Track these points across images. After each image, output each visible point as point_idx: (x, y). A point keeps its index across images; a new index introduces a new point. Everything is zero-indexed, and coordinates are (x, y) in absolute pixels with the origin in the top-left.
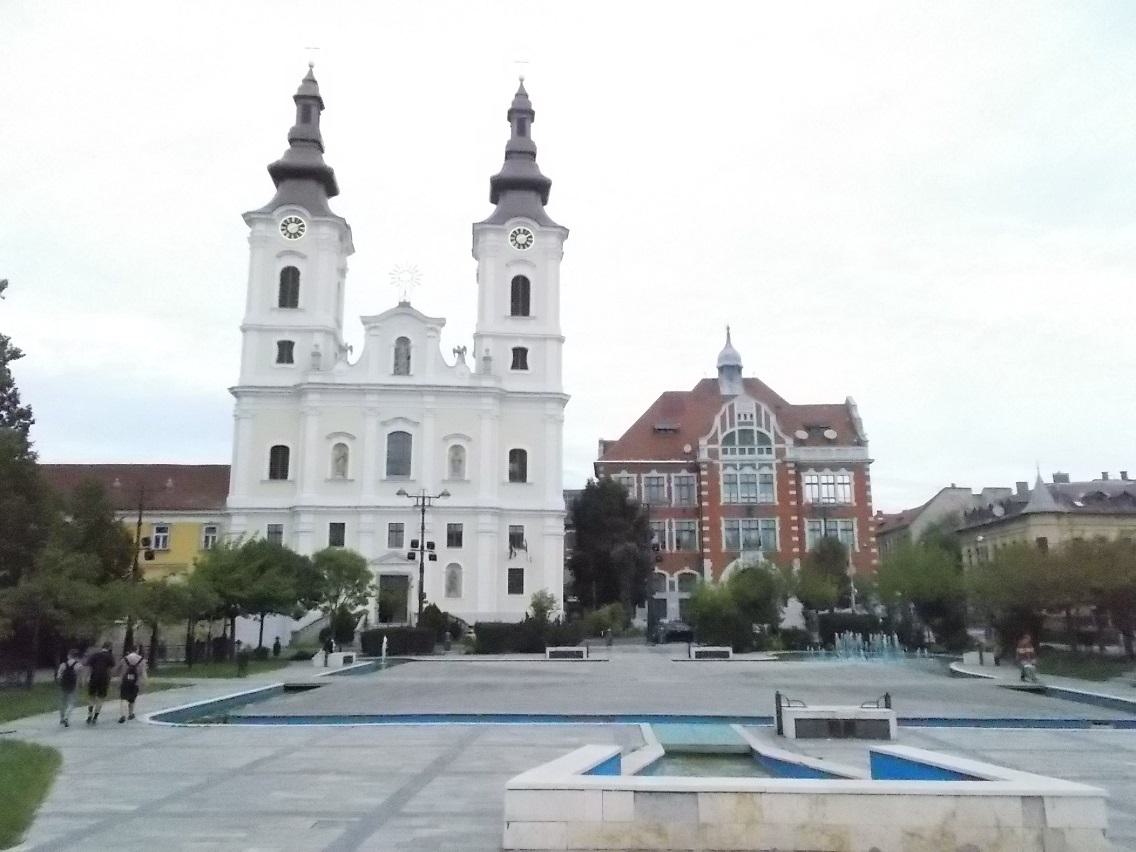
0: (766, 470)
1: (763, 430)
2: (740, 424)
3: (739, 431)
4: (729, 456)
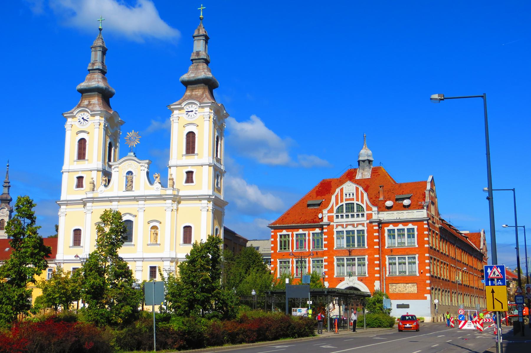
0: (360, 228)
1: (360, 203)
2: (346, 200)
3: (346, 204)
4: (340, 220)
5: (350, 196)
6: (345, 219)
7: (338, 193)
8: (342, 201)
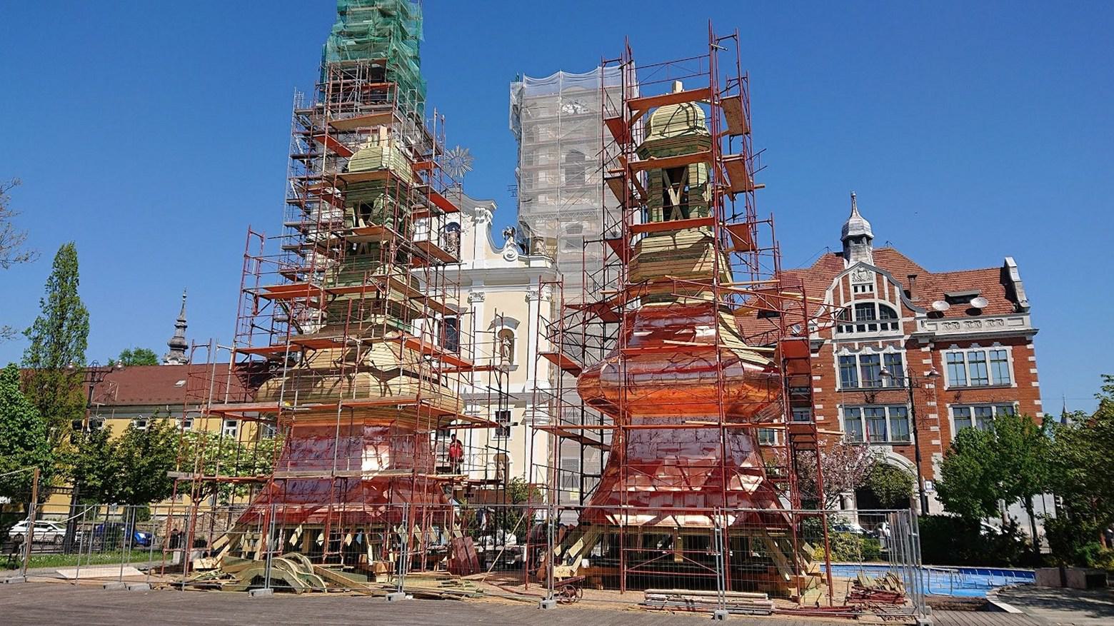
1: (887, 303)
2: (857, 297)
4: (845, 335)
5: (864, 290)
6: (856, 334)
7: (838, 286)
8: (847, 299)
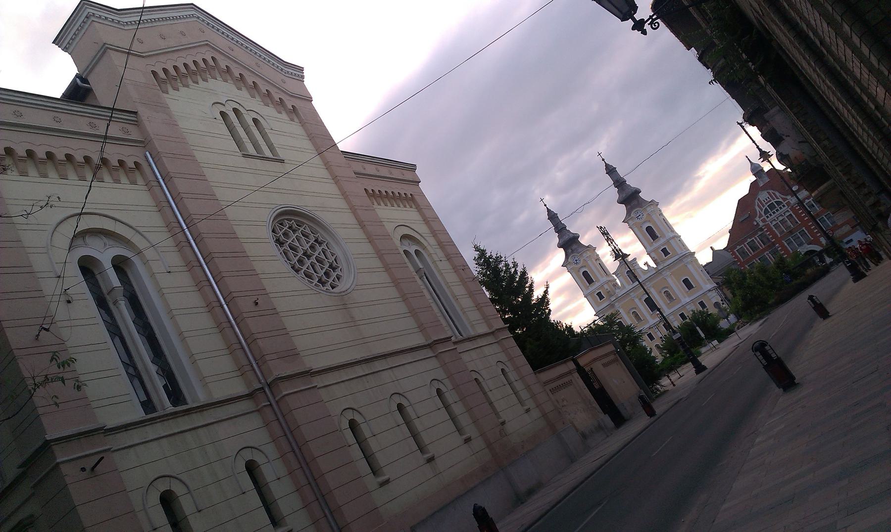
0: (788, 214)
2: (766, 203)
4: (770, 218)
6: (773, 216)
8: (764, 206)
